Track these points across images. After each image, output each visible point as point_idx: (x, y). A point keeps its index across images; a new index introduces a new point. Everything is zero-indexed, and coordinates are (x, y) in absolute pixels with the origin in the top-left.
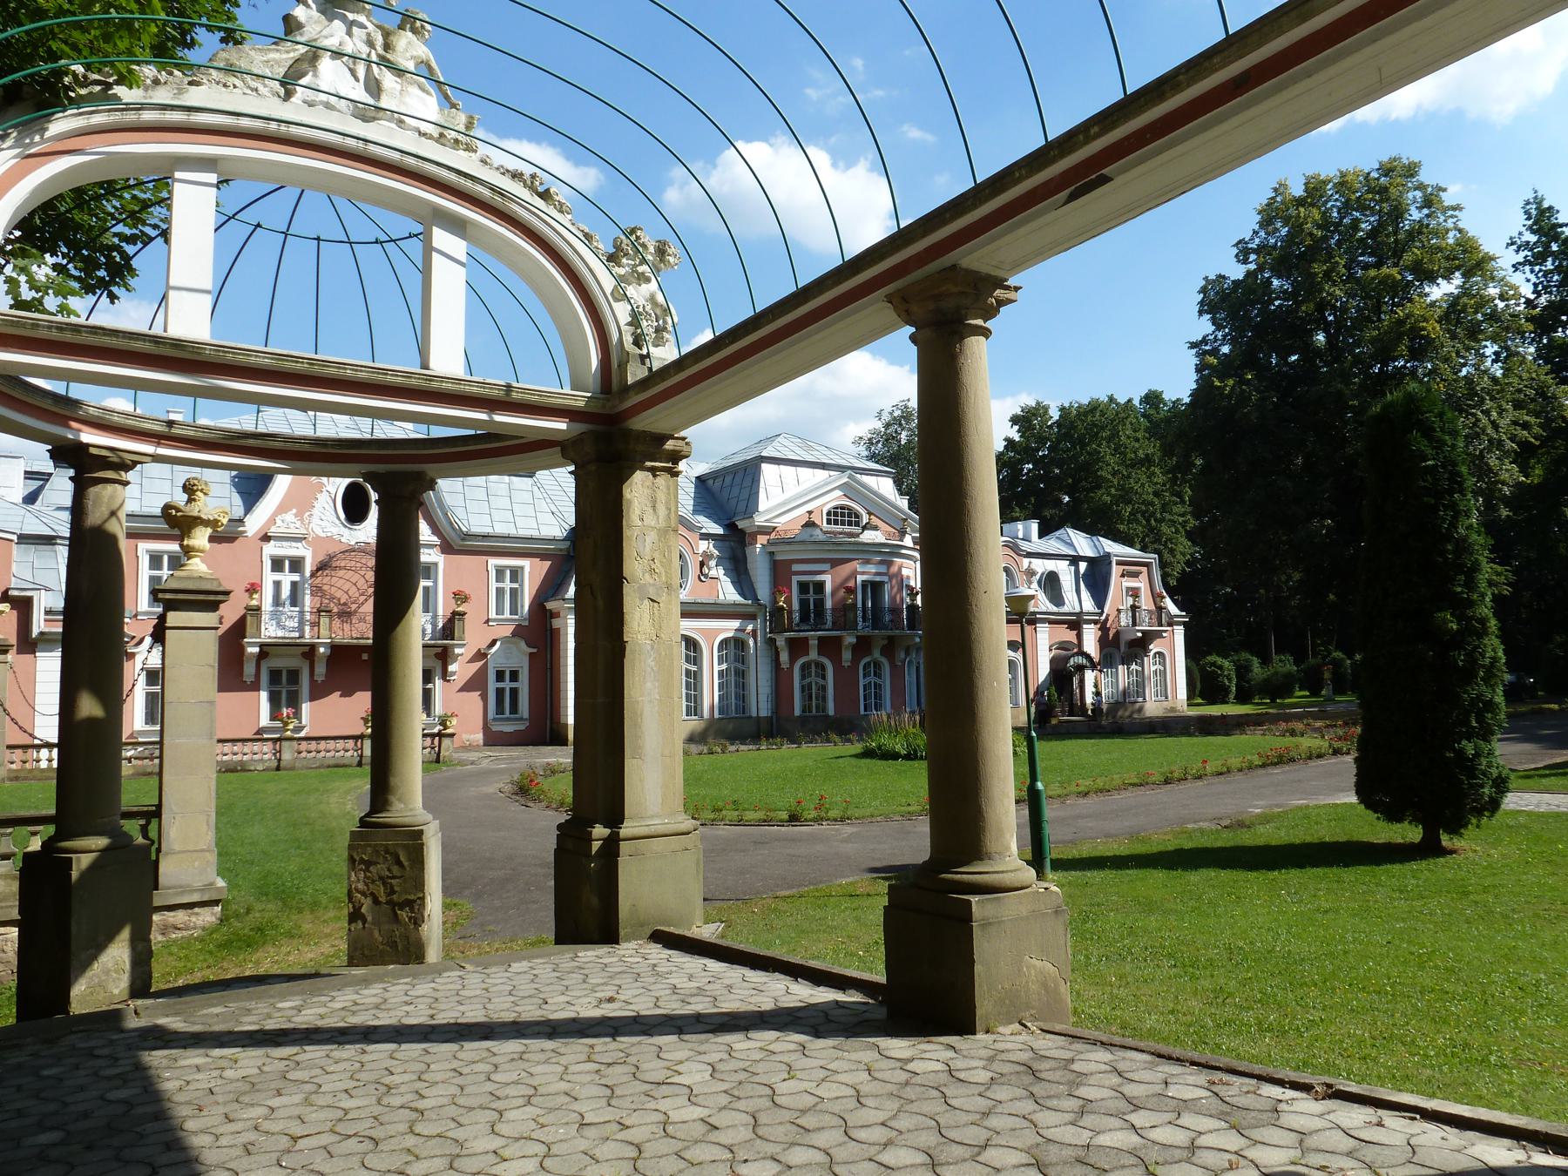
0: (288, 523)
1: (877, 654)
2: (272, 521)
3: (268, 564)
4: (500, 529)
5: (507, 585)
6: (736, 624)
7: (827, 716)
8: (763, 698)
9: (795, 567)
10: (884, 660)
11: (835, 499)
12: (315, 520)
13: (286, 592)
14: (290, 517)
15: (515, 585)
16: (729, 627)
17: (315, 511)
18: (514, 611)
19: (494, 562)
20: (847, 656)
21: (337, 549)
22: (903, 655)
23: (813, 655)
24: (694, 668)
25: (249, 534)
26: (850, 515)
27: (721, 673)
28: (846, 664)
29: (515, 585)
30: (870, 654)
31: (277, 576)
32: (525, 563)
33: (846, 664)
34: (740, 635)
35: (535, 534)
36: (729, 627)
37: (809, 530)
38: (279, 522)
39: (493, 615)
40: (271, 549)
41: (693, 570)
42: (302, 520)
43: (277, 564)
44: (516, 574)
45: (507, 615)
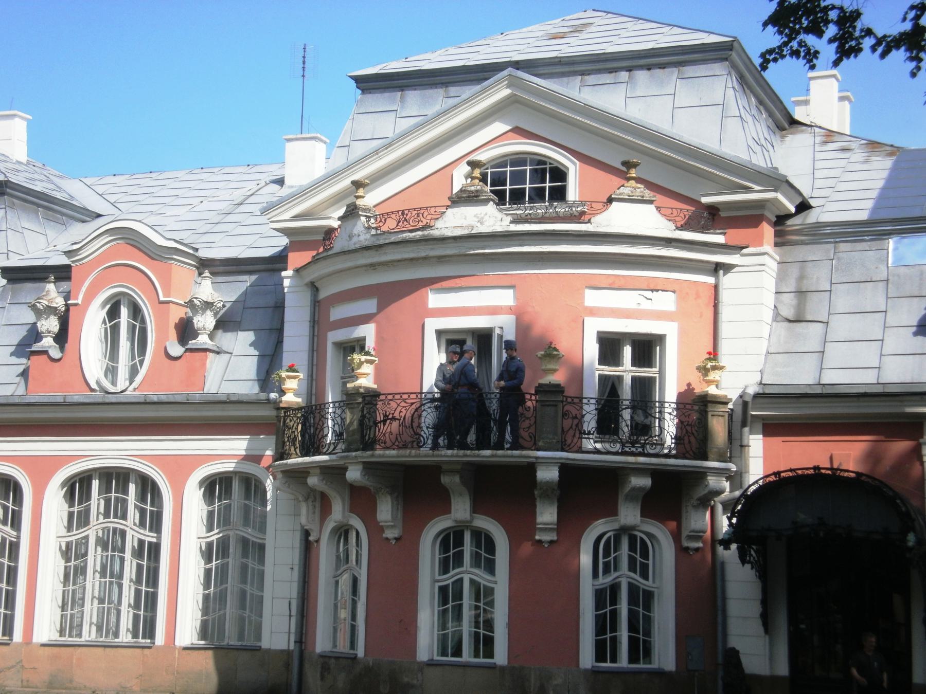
1: (461, 509)
6: (238, 445)
7: (354, 658)
8: (282, 608)
9: (338, 313)
10: (485, 523)
11: (493, 142)
16: (227, 451)
20: (385, 511)
22: (547, 515)
23: (338, 512)
24: (149, 537)
26: (539, 175)
27: (207, 554)
28: (390, 534)
30: (447, 510)
33: (390, 534)
34: (250, 468)
36: (227, 451)
37: (349, 224)
41: (160, 336)
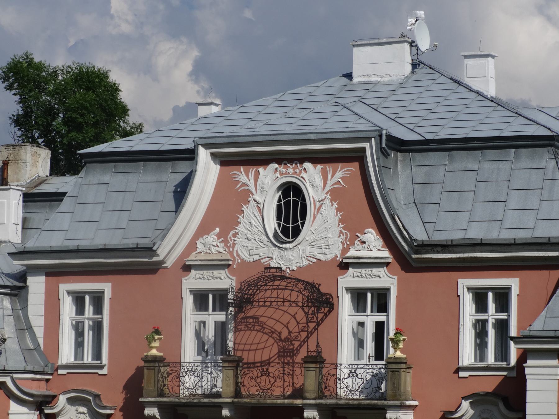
0: (211, 246)
2: (192, 246)
3: (189, 301)
4: (475, 233)
5: (492, 314)
12: (240, 240)
13: (210, 333)
14: (211, 238)
15: (503, 316)
17: (241, 229)
18: (502, 353)
19: (466, 283)
21: (253, 274)
25: (169, 263)
29: (503, 316)
31: (202, 316)
32: (513, 283)
35: (522, 235)
38: (200, 247)
39: (468, 357)
40: (194, 281)
42: (225, 242)
43: (201, 299)
44: (502, 297)
45: (491, 359)
